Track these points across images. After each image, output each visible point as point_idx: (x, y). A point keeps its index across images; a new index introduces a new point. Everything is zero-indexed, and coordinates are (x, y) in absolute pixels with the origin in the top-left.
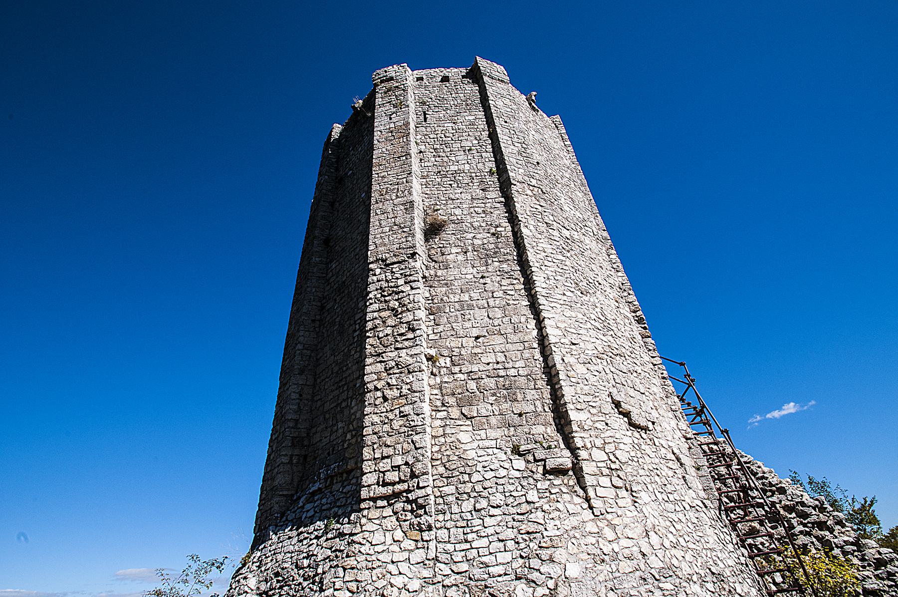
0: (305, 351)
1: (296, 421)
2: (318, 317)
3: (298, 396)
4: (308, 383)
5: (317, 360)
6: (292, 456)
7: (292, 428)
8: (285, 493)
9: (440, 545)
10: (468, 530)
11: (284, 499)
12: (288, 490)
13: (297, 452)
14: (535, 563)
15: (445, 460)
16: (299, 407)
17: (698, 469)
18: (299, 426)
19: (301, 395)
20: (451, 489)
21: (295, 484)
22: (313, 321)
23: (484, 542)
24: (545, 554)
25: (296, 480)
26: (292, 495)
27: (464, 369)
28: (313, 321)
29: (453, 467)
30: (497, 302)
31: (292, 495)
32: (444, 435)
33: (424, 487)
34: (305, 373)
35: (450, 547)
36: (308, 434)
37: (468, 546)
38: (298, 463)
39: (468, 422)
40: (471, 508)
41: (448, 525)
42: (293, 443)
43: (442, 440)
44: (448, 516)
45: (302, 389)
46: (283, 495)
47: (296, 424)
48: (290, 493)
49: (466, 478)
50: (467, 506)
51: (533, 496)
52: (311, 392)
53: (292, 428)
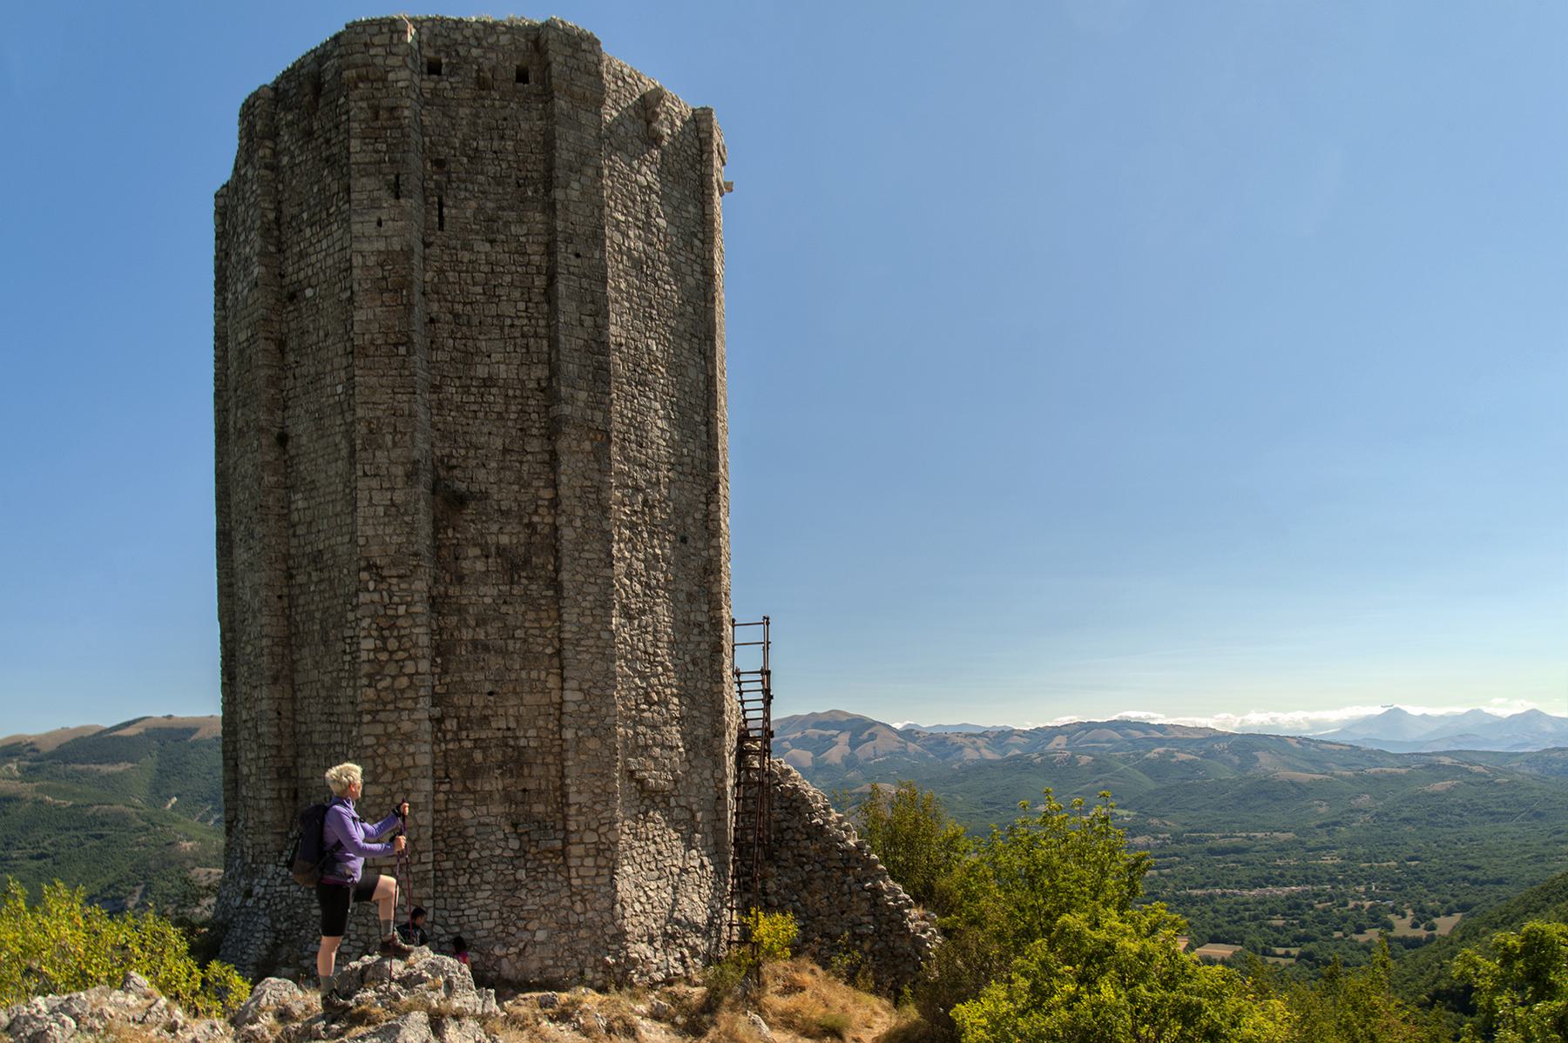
0: (275, 649)
1: (278, 747)
2: (285, 590)
3: (275, 715)
4: (286, 696)
5: (294, 662)
6: (280, 790)
7: (276, 756)
8: (279, 830)
9: (438, 913)
10: (462, 901)
11: (278, 837)
12: (282, 827)
13: (285, 785)
14: (513, 930)
15: (446, 835)
16: (280, 729)
17: (684, 540)
18: (282, 753)
19: (279, 713)
20: (448, 865)
21: (288, 821)
22: (280, 597)
23: (475, 911)
24: (521, 924)
25: (289, 815)
26: (287, 833)
27: (472, 736)
28: (280, 597)
29: (453, 843)
30: (518, 646)
31: (287, 833)
32: (446, 811)
33: (424, 863)
34: (280, 682)
35: (446, 913)
36: (294, 763)
37: (461, 913)
38: (288, 797)
39: (472, 796)
40: (465, 882)
41: (445, 895)
42: (279, 775)
43: (444, 814)
44: (445, 889)
45: (280, 704)
46: (278, 833)
47: (279, 751)
48: (284, 830)
49: (464, 854)
50: (463, 880)
51: (521, 874)
52: (290, 707)
53: (276, 756)
